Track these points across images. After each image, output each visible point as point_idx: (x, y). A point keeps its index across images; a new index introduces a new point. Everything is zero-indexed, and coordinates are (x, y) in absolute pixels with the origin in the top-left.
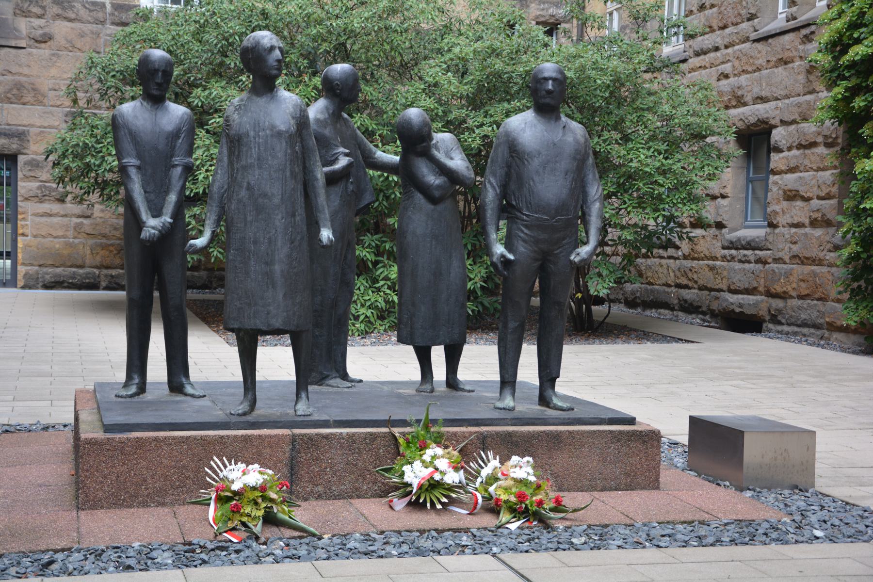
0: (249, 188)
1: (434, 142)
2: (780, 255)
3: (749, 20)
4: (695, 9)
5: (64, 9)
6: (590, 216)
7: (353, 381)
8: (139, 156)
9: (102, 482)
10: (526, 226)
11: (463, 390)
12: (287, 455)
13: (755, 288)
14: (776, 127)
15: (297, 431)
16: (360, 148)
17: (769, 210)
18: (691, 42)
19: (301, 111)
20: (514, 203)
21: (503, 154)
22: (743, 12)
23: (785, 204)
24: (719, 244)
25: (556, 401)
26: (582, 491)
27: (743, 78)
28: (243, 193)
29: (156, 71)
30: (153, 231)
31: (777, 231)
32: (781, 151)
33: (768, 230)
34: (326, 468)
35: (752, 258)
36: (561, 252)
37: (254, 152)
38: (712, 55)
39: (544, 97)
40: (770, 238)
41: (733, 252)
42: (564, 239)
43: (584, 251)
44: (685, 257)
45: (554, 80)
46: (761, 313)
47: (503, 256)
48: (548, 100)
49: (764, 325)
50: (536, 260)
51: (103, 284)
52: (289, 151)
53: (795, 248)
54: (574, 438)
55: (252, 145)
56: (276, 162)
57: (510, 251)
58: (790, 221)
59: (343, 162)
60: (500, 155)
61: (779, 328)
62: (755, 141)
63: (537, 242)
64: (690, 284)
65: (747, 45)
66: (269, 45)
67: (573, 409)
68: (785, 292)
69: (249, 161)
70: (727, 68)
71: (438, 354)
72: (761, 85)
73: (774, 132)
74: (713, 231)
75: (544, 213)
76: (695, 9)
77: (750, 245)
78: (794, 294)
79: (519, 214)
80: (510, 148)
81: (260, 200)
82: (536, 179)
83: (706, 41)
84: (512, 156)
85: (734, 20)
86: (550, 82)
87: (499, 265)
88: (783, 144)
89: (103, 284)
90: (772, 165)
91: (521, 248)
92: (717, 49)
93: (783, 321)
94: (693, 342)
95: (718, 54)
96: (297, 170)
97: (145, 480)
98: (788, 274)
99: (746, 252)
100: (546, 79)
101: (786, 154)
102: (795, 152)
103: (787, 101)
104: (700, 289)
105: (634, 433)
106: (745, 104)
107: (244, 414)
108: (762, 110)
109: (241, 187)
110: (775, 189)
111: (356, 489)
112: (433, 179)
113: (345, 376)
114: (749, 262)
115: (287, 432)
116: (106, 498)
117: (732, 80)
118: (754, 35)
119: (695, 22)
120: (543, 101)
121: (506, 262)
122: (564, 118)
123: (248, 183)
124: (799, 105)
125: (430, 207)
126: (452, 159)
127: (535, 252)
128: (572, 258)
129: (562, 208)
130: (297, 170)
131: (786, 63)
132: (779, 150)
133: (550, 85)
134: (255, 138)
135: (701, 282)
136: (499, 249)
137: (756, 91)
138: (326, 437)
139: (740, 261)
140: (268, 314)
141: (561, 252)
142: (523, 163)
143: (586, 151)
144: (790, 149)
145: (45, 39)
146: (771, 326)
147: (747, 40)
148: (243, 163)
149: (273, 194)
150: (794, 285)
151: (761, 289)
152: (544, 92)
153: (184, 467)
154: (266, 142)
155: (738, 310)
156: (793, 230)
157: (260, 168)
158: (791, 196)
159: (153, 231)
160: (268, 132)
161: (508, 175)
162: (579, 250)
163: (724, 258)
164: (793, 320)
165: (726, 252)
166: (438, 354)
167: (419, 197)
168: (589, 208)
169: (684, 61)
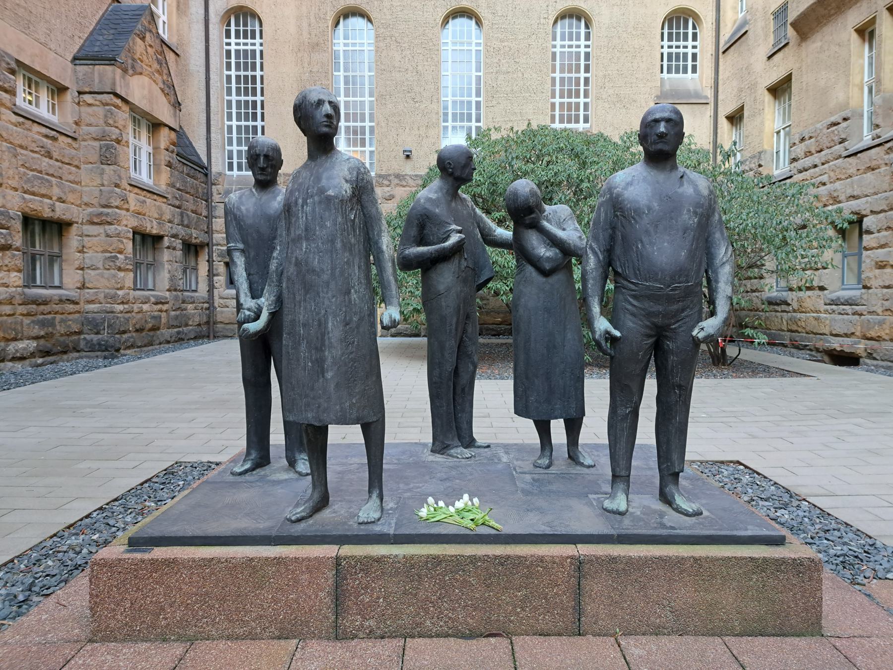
0: (298, 264)
1: (545, 214)
2: (874, 309)
3: (840, 143)
4: (797, 142)
5: (400, 180)
6: (717, 282)
7: (479, 447)
8: (244, 243)
9: (114, 610)
10: (635, 297)
11: (582, 464)
12: (330, 582)
13: (853, 333)
14: (866, 216)
15: (348, 550)
16: (479, 227)
17: (863, 276)
18: (795, 164)
19: (358, 174)
20: (620, 270)
21: (606, 214)
22: (836, 138)
23: (877, 271)
24: (822, 302)
25: (680, 501)
26: (713, 635)
27: (838, 185)
28: (292, 269)
29: (258, 156)
30: (247, 313)
31: (870, 291)
32: (872, 233)
33: (863, 291)
34: (379, 598)
35: (850, 312)
36: (680, 327)
37: (302, 222)
38: (812, 171)
39: (655, 143)
40: (865, 297)
41: (834, 307)
42: (683, 310)
43: (710, 326)
44: (794, 311)
45: (668, 120)
46: (858, 351)
47: (607, 332)
48: (660, 146)
49: (861, 360)
50: (649, 336)
51: (423, 334)
52: (340, 219)
53: (887, 304)
54: (701, 566)
55: (300, 215)
56: (324, 232)
57: (615, 328)
58: (882, 284)
59: (454, 239)
60: (603, 215)
61: (875, 362)
62: (853, 228)
63: (649, 315)
64: (800, 330)
65: (840, 160)
66: (316, 99)
67: (701, 513)
68: (879, 337)
69: (297, 233)
70: (824, 178)
71: (558, 428)
72: (853, 187)
73: (865, 219)
74: (817, 292)
75: (656, 281)
76: (797, 142)
77: (849, 302)
78: (887, 338)
79: (625, 283)
80: (614, 207)
81: (308, 277)
82: (645, 239)
83: (807, 162)
84: (617, 216)
85: (829, 145)
86: (663, 124)
87: (603, 343)
88: (873, 228)
89: (423, 334)
90: (864, 244)
91: (630, 323)
92: (815, 166)
93: (878, 358)
94: (805, 375)
95: (817, 169)
96: (353, 240)
97: (162, 609)
98: (881, 323)
99: (844, 307)
100: (657, 121)
101: (876, 235)
102: (884, 233)
103: (876, 197)
104: (807, 333)
105: (783, 561)
106: (840, 202)
107: (299, 520)
108: (854, 205)
109: (290, 262)
110: (868, 261)
111: (417, 625)
112: (543, 251)
113: (470, 442)
114: (847, 314)
115: (329, 551)
116: (119, 628)
117: (828, 186)
118: (845, 154)
119: (799, 150)
120: (653, 148)
121: (613, 340)
122: (681, 169)
123: (296, 258)
124: (886, 198)
125: (541, 279)
126: (564, 230)
127: (647, 326)
128: (694, 333)
129: (681, 273)
130: (353, 240)
131: (873, 170)
132: (869, 232)
133: (662, 128)
134: (303, 207)
135: (808, 329)
136: (602, 324)
137: (849, 192)
138: (379, 560)
139: (840, 314)
140: (319, 407)
141: (680, 327)
142: (630, 222)
143: (710, 205)
144: (879, 231)
145: (391, 198)
146: (868, 361)
147: (840, 157)
148: (293, 235)
149: (322, 270)
150: (887, 331)
151: (858, 333)
152: (656, 137)
153: (207, 593)
154: (314, 210)
155: (839, 349)
156: (885, 290)
157: (307, 239)
158: (881, 266)
159: (247, 313)
160: (316, 198)
161: (612, 238)
162: (703, 324)
163: (826, 311)
164: (886, 357)
165: (828, 307)
166: (558, 428)
167: (530, 270)
168: (716, 272)
169: (791, 177)
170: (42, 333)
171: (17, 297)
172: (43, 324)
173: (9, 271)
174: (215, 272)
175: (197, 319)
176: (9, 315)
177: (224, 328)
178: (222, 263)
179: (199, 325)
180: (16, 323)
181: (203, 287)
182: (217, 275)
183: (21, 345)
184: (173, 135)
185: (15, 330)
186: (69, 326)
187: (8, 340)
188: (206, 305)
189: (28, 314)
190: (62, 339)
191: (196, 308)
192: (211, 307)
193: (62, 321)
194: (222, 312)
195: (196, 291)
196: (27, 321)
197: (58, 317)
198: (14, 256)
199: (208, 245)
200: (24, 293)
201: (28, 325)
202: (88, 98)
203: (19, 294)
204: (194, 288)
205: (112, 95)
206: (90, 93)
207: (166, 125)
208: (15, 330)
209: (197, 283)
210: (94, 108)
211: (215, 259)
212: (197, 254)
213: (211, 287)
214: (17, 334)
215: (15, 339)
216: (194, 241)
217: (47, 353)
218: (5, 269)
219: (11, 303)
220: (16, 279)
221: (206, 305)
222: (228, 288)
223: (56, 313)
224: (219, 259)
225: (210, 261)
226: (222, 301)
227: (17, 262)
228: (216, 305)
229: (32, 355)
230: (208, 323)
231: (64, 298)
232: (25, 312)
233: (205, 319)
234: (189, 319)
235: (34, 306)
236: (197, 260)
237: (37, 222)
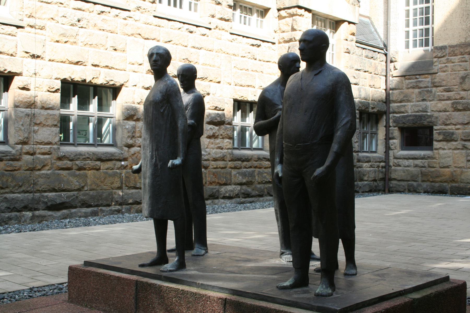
170: (244, 181)
171: (228, 156)
172: (244, 175)
173: (223, 138)
174: (391, 136)
175: (372, 176)
176: (222, 168)
177: (396, 185)
178: (396, 128)
179: (375, 180)
180: (226, 173)
181: (381, 148)
182: (393, 138)
183: (229, 188)
184: (353, 28)
185: (226, 178)
186: (265, 177)
187: (221, 185)
188: (383, 164)
189: (235, 168)
190: (259, 186)
191: (371, 166)
192: (387, 166)
193: (259, 173)
194: (395, 171)
195: (375, 152)
196: (234, 172)
197: (257, 170)
198: (226, 128)
199: (385, 113)
200: (232, 154)
201: (235, 175)
202: (283, 13)
203: (230, 154)
204: (374, 149)
205: (296, 9)
206: (284, 9)
207: (344, 21)
208: (226, 178)
209: (377, 145)
210: (287, 19)
211: (391, 124)
212: (377, 122)
213: (388, 148)
214: (226, 180)
215: (225, 184)
216: (371, 110)
217: (247, 195)
218: (221, 137)
219: (224, 160)
220: (228, 144)
221: (383, 164)
222: (402, 149)
223: (256, 167)
224: (394, 124)
225: (387, 127)
226: (396, 161)
227: (228, 132)
228: (391, 164)
229: (237, 196)
230: (383, 179)
231: (261, 157)
232: (233, 166)
233: (381, 176)
234: (364, 175)
235: (240, 162)
236: (377, 126)
237: (248, 104)
